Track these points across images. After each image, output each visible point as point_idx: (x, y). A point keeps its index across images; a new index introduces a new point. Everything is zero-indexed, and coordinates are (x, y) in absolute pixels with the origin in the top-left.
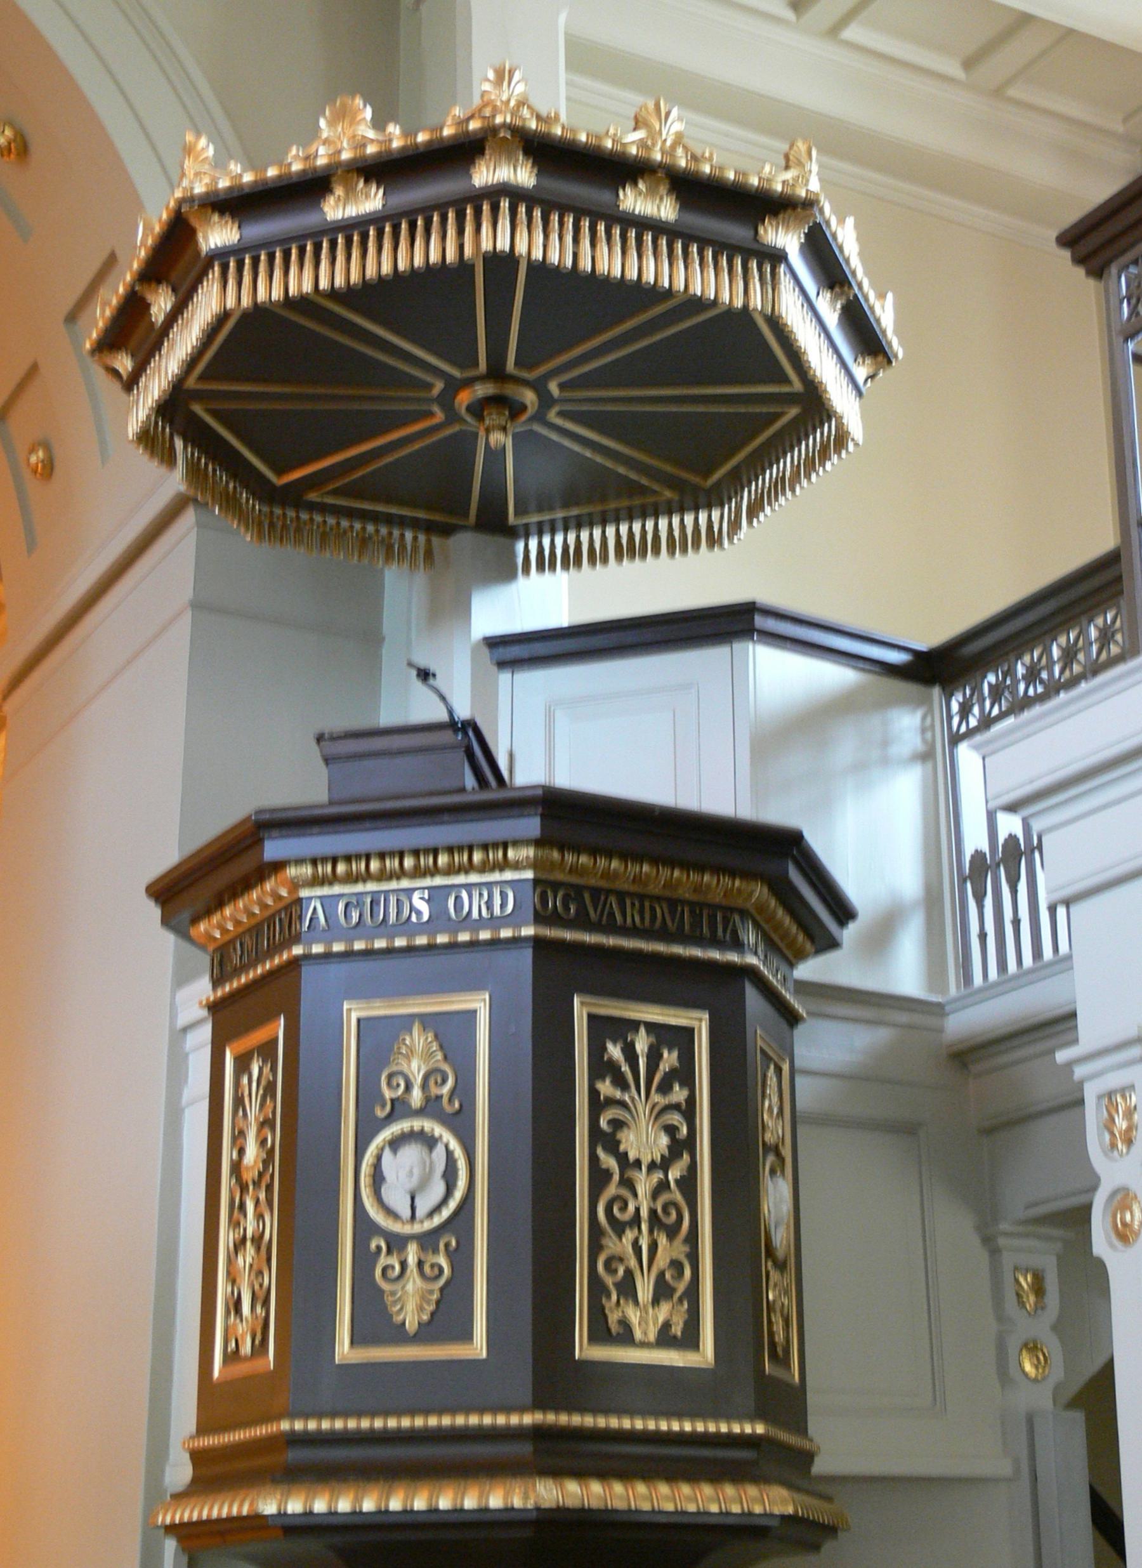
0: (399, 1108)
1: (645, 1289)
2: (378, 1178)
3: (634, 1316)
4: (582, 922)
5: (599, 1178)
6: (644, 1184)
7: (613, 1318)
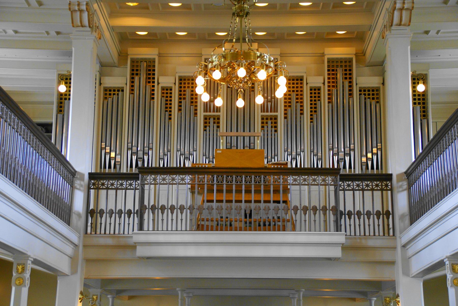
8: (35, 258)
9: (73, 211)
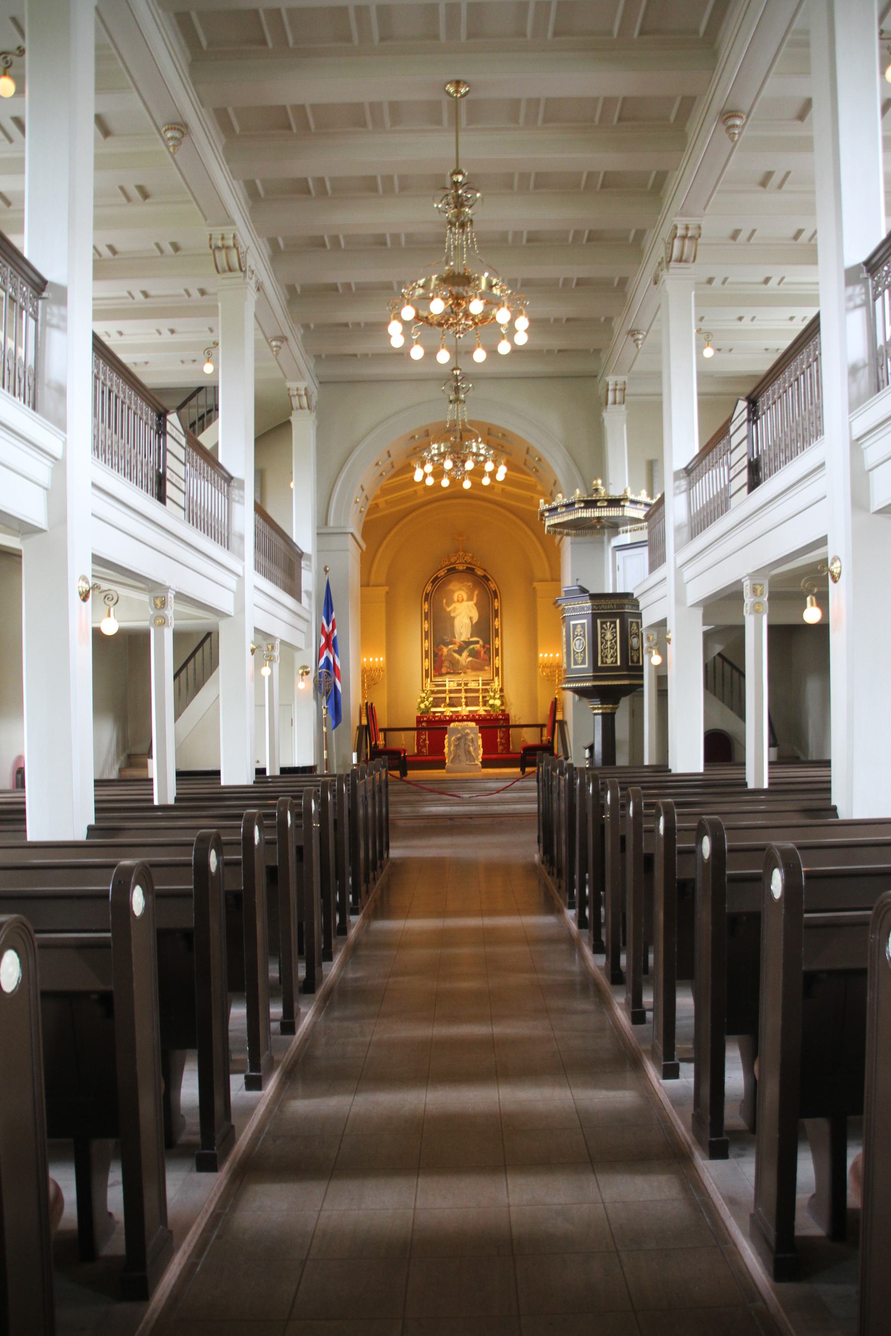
0: (577, 636)
1: (609, 656)
2: (575, 645)
3: (608, 660)
4: (598, 609)
5: (602, 643)
6: (609, 643)
7: (604, 662)
8: (177, 590)
9: (233, 532)
